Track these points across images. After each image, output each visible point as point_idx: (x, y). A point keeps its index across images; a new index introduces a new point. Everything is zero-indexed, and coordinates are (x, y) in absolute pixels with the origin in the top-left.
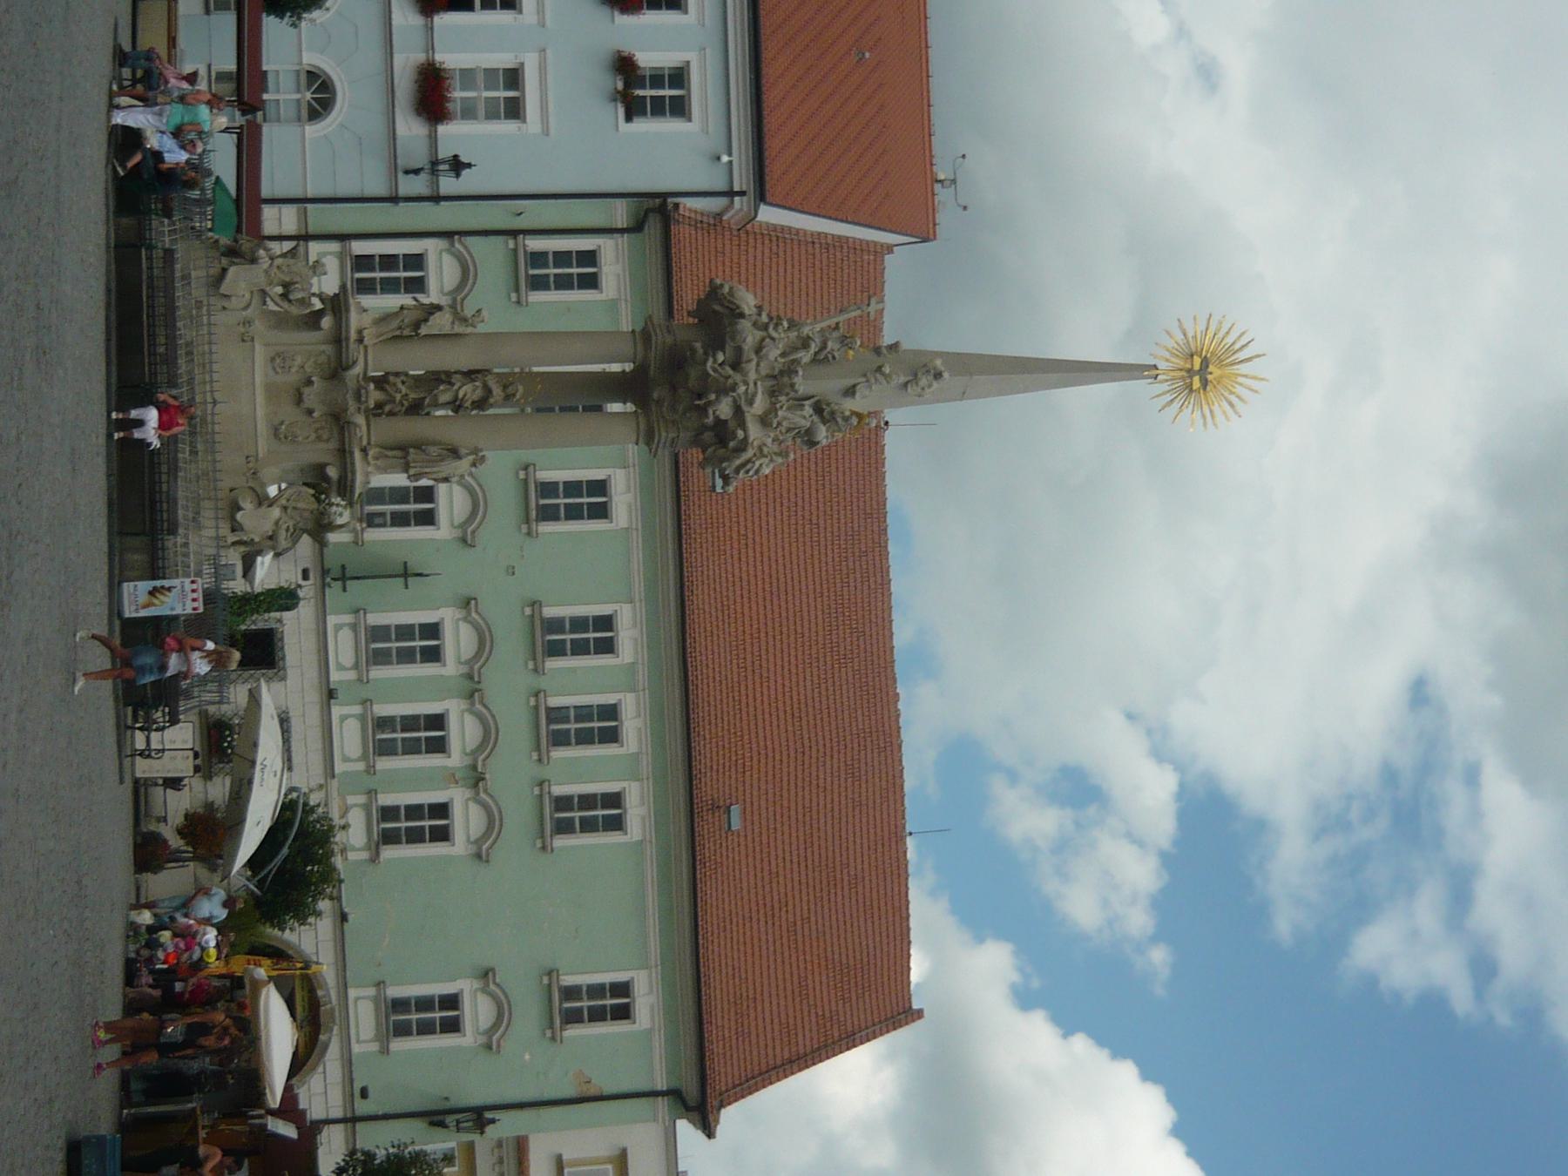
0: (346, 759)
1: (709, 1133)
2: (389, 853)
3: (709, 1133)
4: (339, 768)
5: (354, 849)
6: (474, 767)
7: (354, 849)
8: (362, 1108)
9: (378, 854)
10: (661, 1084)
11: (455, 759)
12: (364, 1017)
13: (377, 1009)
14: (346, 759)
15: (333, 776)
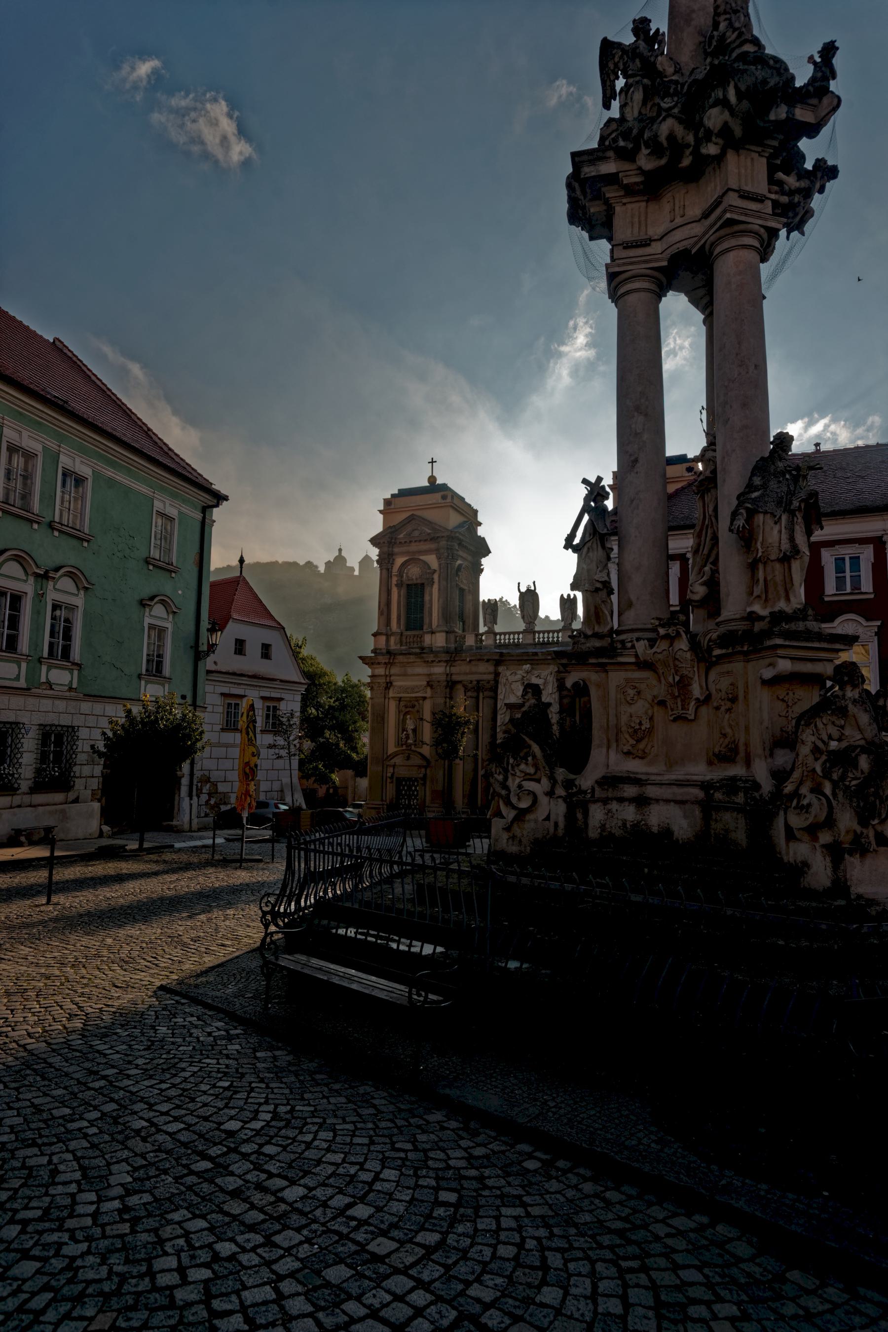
0: (18, 678)
1: (226, 498)
2: (76, 653)
3: (226, 498)
4: (22, 683)
5: (71, 682)
6: (37, 575)
7: (71, 682)
8: (189, 700)
9: (77, 664)
10: (199, 516)
11: (28, 588)
12: (151, 691)
13: (151, 682)
14: (18, 678)
15: (29, 689)
